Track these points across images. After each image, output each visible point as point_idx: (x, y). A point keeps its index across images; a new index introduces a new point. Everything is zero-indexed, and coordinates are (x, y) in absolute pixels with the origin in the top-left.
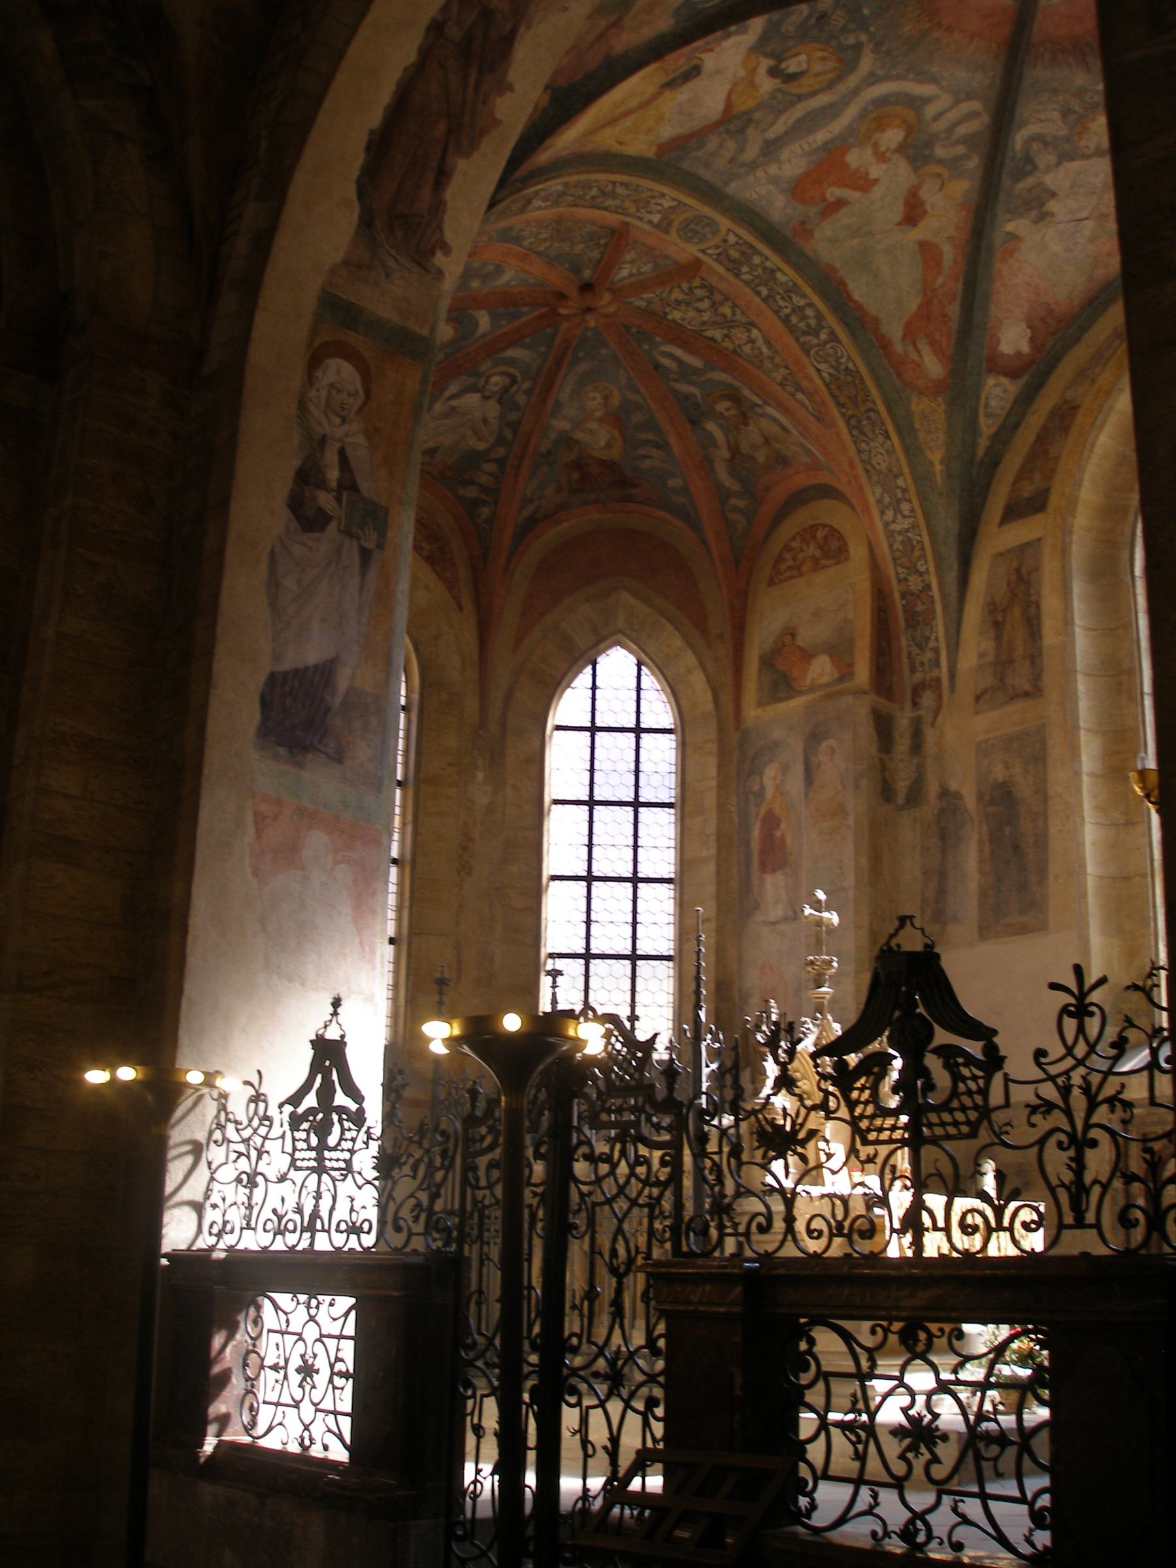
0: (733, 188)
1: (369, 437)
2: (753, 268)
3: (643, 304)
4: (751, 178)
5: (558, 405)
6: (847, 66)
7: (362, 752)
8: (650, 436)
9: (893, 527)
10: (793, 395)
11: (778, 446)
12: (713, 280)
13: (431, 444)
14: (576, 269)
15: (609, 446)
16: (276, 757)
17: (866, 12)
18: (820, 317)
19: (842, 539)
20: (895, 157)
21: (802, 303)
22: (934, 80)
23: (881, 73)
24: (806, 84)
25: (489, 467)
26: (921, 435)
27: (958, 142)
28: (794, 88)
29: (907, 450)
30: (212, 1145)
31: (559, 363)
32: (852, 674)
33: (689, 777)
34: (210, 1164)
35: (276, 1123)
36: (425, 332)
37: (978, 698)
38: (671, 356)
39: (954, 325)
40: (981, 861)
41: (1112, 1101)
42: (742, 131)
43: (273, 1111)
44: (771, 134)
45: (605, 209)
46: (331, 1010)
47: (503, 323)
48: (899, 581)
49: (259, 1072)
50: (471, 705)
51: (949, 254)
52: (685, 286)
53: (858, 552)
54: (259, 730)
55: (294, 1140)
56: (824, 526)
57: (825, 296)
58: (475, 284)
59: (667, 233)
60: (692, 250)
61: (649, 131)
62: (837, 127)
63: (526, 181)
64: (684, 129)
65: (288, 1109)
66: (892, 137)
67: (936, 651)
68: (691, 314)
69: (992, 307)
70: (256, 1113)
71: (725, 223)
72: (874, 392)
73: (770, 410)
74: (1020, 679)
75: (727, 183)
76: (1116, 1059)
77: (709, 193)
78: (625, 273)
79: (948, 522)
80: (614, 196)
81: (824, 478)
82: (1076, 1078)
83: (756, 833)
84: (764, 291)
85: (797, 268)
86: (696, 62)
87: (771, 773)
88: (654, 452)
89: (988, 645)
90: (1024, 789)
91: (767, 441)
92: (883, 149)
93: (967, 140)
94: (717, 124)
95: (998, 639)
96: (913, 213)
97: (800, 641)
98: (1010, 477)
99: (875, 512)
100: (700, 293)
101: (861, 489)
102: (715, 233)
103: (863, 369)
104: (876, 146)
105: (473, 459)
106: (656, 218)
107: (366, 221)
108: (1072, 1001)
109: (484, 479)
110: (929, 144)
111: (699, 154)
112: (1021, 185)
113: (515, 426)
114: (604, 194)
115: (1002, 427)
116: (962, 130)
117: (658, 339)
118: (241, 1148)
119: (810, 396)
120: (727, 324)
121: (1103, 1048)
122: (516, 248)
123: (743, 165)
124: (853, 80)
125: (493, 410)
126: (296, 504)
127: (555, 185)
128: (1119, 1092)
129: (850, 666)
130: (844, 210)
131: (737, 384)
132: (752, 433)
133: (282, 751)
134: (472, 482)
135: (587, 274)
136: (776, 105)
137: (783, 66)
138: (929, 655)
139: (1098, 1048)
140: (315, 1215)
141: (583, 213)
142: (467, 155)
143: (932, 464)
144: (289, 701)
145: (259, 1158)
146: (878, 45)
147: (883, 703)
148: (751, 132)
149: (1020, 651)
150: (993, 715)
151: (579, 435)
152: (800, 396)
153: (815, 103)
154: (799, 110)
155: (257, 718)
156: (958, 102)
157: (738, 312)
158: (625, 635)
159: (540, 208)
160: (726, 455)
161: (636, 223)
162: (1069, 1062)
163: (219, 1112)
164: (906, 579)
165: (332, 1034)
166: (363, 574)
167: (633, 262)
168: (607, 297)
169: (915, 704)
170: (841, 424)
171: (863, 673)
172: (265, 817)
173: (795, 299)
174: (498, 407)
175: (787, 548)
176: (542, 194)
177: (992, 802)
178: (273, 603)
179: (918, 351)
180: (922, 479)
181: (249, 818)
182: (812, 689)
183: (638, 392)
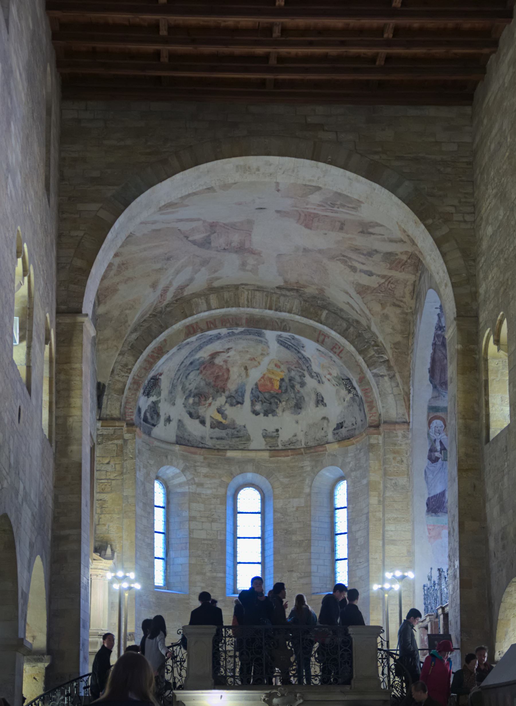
16: (432, 516)
107: (435, 387)
133: (433, 514)
155: (425, 508)
178: (427, 482)
181: (426, 530)
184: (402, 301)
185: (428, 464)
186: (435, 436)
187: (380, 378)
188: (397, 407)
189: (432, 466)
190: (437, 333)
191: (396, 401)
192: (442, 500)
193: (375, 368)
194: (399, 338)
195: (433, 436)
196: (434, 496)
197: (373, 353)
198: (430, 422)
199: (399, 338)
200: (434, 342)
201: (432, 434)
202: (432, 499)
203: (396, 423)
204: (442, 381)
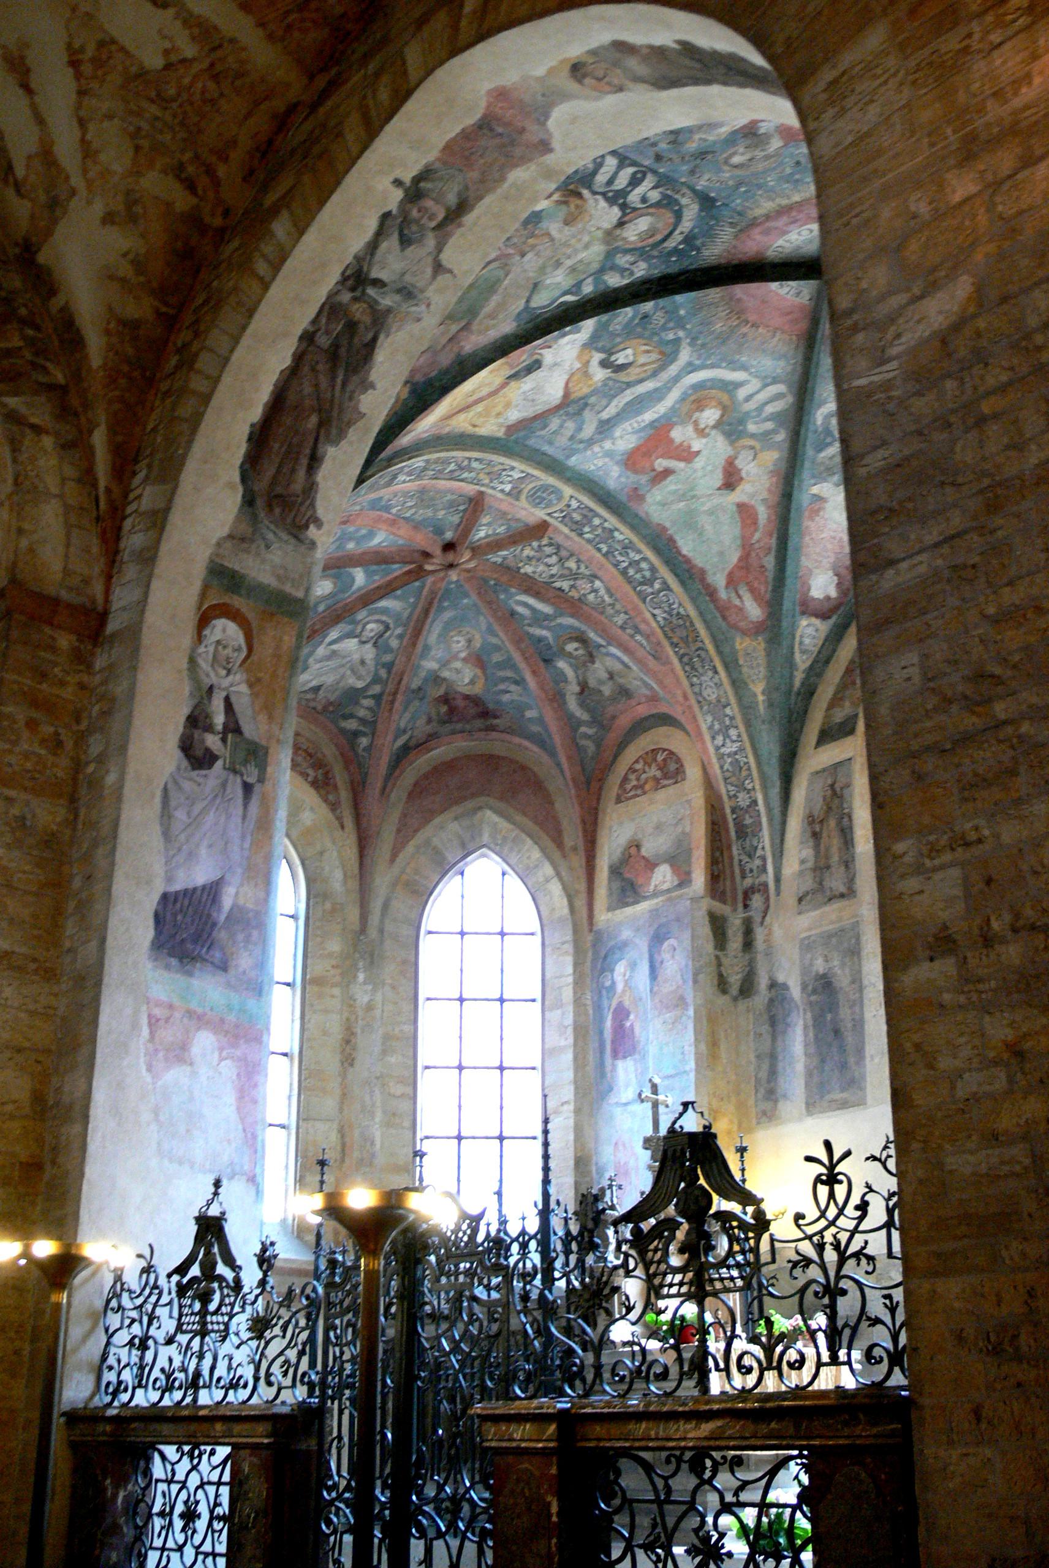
0: (573, 461)
1: (251, 686)
2: (594, 528)
3: (499, 560)
4: (589, 453)
5: (427, 648)
6: (668, 356)
7: (244, 961)
8: (509, 674)
9: (723, 750)
10: (632, 636)
11: (621, 681)
12: (559, 539)
13: (314, 683)
14: (439, 531)
15: (472, 682)
16: (168, 967)
17: (682, 312)
18: (653, 569)
19: (678, 761)
20: (713, 432)
21: (637, 557)
22: (744, 368)
23: (697, 362)
24: (633, 373)
25: (366, 702)
26: (745, 670)
27: (768, 419)
28: (623, 377)
29: (733, 683)
30: (109, 1313)
31: (426, 612)
32: (690, 881)
33: (548, 975)
34: (107, 1330)
35: (166, 1291)
36: (300, 594)
37: (800, 900)
38: (526, 605)
39: (770, 575)
40: (806, 1045)
41: (857, 1255)
42: (579, 413)
43: (162, 1281)
44: (605, 415)
45: (462, 480)
46: (213, 1190)
47: (376, 578)
48: (730, 797)
49: (151, 1246)
50: (353, 914)
51: (763, 514)
52: (535, 544)
53: (693, 772)
54: (153, 943)
55: (181, 1307)
56: (664, 750)
57: (657, 550)
58: (351, 546)
59: (517, 499)
60: (540, 514)
61: (499, 414)
62: (661, 408)
63: (390, 462)
64: (529, 413)
65: (175, 1278)
66: (710, 415)
67: (764, 859)
68: (541, 568)
69: (803, 558)
70: (147, 1283)
71: (568, 491)
72: (703, 632)
73: (613, 650)
74: (836, 882)
75: (568, 457)
76: (861, 1219)
77: (553, 466)
78: (482, 534)
79: (771, 744)
80: (470, 469)
81: (663, 708)
82: (828, 1237)
83: (609, 1024)
84: (605, 549)
85: (633, 528)
86: (536, 357)
87: (620, 968)
88: (513, 688)
89: (808, 852)
90: (842, 979)
91: (611, 676)
92: (702, 426)
93: (773, 417)
94: (558, 408)
95: (817, 847)
96: (731, 479)
97: (644, 852)
98: (824, 705)
99: (707, 738)
100: (548, 550)
101: (694, 717)
102: (560, 498)
103: (693, 613)
104: (696, 423)
105: (353, 695)
106: (508, 488)
107: (249, 501)
108: (825, 1171)
109: (362, 713)
110: (742, 421)
111: (543, 433)
112: (823, 454)
113: (389, 666)
114: (461, 468)
115: (815, 661)
116: (770, 409)
117: (513, 590)
118: (134, 1314)
119: (647, 637)
120: (575, 576)
121: (850, 1211)
122: (385, 515)
123: (581, 442)
124: (673, 369)
125: (369, 652)
126: (187, 747)
127: (418, 462)
128: (864, 1248)
129: (688, 873)
130: (670, 478)
131: (584, 627)
132: (598, 671)
133: (174, 962)
134: (352, 716)
135: (449, 535)
136: (609, 391)
137: (613, 358)
138: (758, 862)
139: (846, 1212)
140: (198, 1374)
141: (443, 484)
142: (336, 442)
143: (755, 695)
144: (179, 918)
145: (150, 1324)
146: (694, 339)
147: (718, 907)
148: (587, 414)
149: (835, 859)
150: (814, 914)
151: (446, 674)
152: (638, 637)
153: (641, 389)
154: (628, 395)
155: (151, 933)
156: (766, 385)
157: (583, 567)
158: (490, 849)
159: (404, 482)
160: (577, 689)
161: (490, 491)
162: (823, 1223)
163: (115, 1283)
164: (735, 796)
165: (214, 1211)
166: (246, 805)
167: (489, 524)
168: (467, 555)
169: (746, 906)
170: (675, 661)
171: (699, 880)
172: (158, 1020)
173: (632, 554)
174: (374, 650)
175: (632, 770)
176: (406, 470)
177: (815, 991)
178: (166, 834)
179: (739, 597)
180: (747, 708)
181: (144, 1021)
182: (655, 895)
183: (497, 636)
184: (210, 171)
185: (178, 769)
186: (212, 674)
187: (28, 431)
188: (68, 545)
189: (191, 779)
190: (339, 298)
191: (68, 527)
192: (209, 916)
193: (16, 395)
194: (141, 308)
195: (212, 675)
196: (186, 892)
197: (16, 342)
198: (204, 621)
199: (141, 308)
200: (312, 329)
201: (204, 665)
202: (175, 901)
203: (56, 602)
204: (279, 490)
